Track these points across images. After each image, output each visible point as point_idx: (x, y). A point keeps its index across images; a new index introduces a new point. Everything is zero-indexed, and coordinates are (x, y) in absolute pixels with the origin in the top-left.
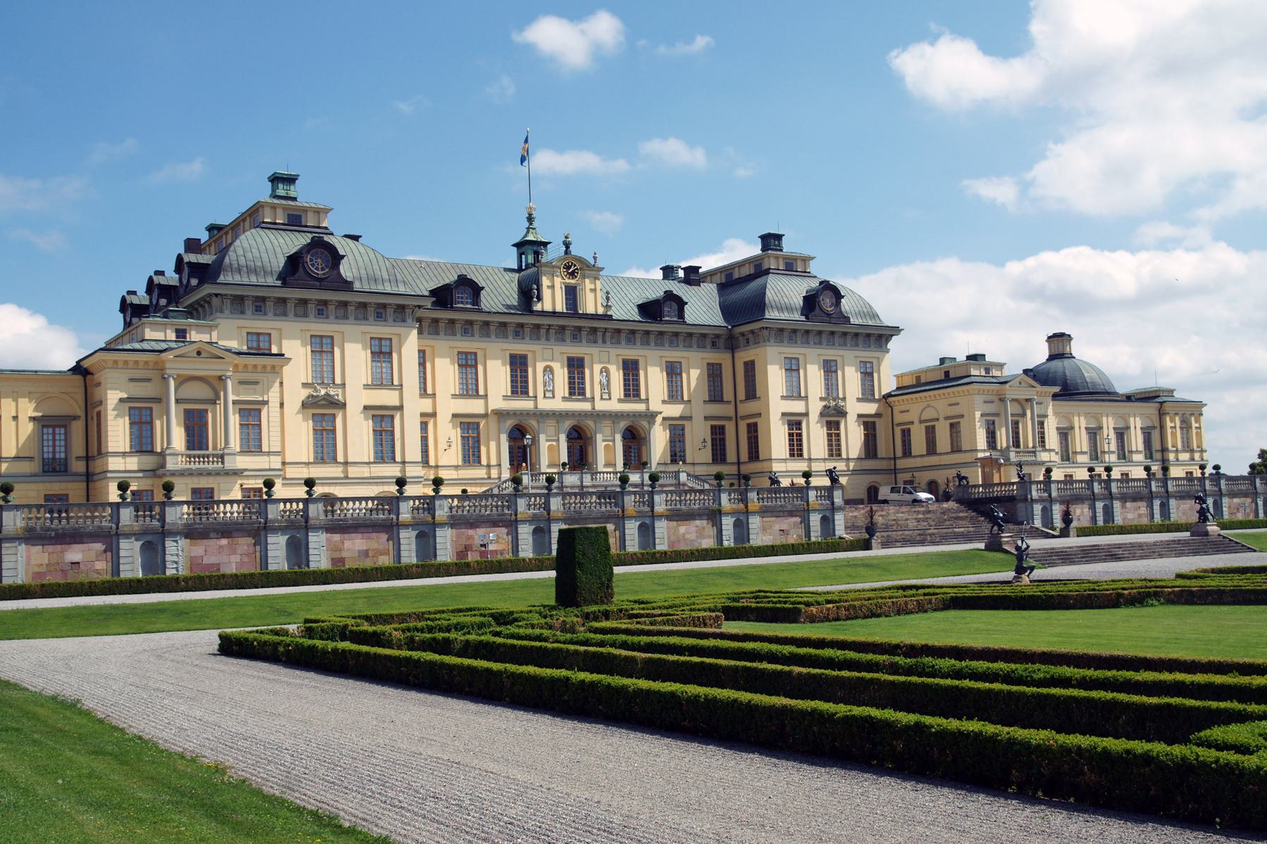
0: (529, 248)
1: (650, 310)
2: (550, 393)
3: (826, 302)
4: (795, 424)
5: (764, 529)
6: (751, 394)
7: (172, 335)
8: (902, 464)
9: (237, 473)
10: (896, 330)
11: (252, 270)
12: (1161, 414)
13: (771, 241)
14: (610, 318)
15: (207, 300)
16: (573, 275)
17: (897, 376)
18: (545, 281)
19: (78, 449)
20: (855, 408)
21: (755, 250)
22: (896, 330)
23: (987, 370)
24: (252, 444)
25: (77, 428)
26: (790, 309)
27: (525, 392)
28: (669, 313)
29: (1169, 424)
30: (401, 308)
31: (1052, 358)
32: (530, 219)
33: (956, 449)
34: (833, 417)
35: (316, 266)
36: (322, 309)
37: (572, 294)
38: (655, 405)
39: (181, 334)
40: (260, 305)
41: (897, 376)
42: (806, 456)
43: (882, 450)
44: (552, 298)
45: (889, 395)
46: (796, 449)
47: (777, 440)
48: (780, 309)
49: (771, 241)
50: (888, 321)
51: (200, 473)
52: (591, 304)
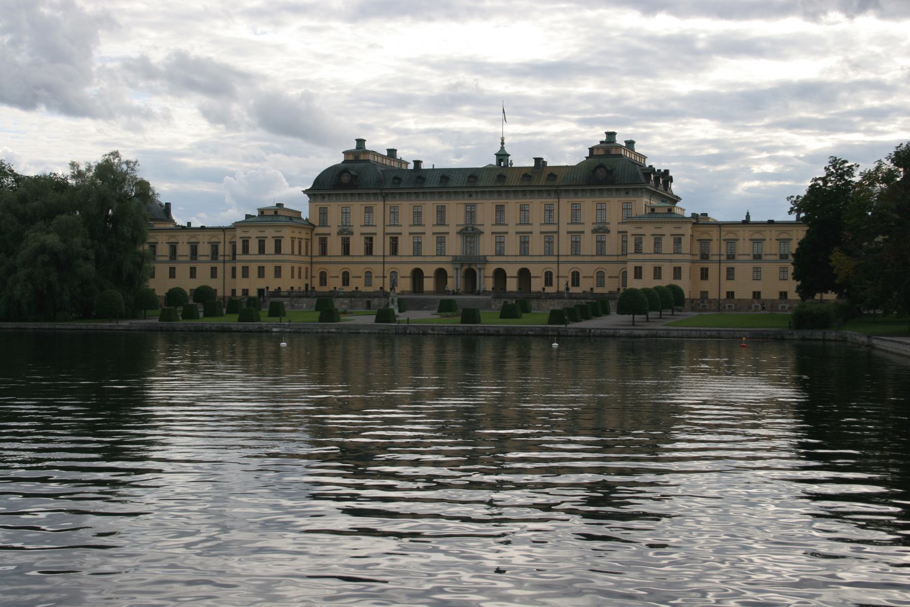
4: (575, 237)
20: (614, 228)
35: (345, 179)
40: (323, 197)
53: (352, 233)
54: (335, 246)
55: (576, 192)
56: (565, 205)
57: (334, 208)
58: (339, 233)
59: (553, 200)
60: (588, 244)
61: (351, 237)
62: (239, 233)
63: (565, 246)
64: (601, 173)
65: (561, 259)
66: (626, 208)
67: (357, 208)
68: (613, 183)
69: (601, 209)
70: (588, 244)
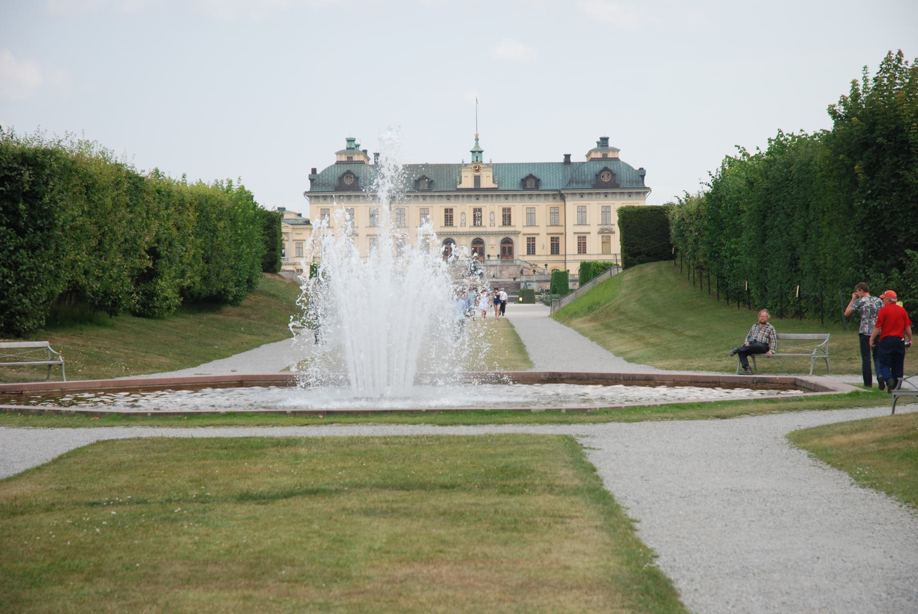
0: (477, 152)
1: (524, 182)
2: (463, 224)
11: (324, 185)
13: (604, 141)
16: (478, 171)
18: (463, 174)
26: (583, 182)
27: (451, 225)
32: (477, 140)
35: (348, 182)
36: (349, 197)
37: (477, 180)
38: (518, 229)
44: (467, 182)
47: (571, 245)
48: (577, 183)
49: (604, 141)
50: (646, 185)
52: (487, 182)
55: (582, 195)
56: (572, 205)
59: (558, 203)
64: (606, 179)
65: (568, 258)
68: (617, 186)
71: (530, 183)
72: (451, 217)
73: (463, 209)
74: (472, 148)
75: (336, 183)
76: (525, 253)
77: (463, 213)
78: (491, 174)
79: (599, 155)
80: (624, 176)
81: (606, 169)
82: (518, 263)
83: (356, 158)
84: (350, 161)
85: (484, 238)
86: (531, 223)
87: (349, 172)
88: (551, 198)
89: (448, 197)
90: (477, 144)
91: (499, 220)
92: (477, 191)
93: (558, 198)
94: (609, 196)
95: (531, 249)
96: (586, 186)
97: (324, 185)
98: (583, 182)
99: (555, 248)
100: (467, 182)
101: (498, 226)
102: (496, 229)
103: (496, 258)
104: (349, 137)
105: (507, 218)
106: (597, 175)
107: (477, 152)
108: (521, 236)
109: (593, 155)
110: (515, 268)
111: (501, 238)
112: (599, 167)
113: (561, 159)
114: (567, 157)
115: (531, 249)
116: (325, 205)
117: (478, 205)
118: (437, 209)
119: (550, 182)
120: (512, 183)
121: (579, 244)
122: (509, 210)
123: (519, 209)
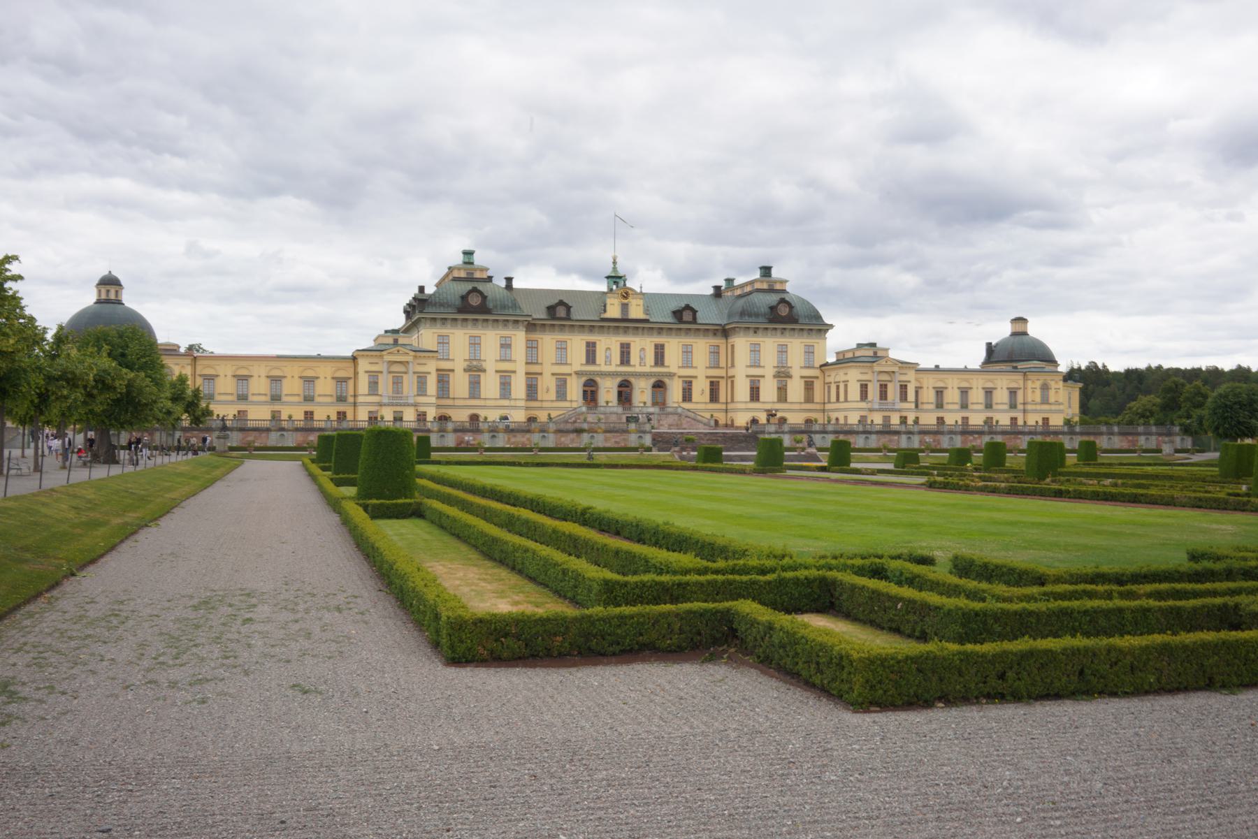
1: (678, 314)
2: (608, 361)
3: (783, 311)
5: (606, 440)
6: (733, 366)
7: (391, 341)
8: (828, 406)
9: (415, 405)
10: (831, 326)
11: (442, 305)
12: (1025, 380)
13: (766, 271)
14: (646, 321)
15: (419, 320)
17: (837, 353)
18: (609, 301)
19: (351, 392)
20: (797, 371)
21: (757, 275)
22: (831, 326)
23: (875, 353)
24: (422, 391)
25: (351, 383)
26: (757, 315)
28: (687, 316)
29: (1030, 384)
30: (516, 322)
31: (1014, 334)
32: (615, 263)
33: (846, 400)
34: (783, 375)
35: (475, 301)
37: (625, 307)
39: (396, 341)
41: (837, 353)
42: (762, 399)
43: (818, 396)
45: (826, 364)
46: (755, 394)
48: (750, 315)
50: (827, 321)
51: (397, 405)
52: (636, 312)
53: (485, 371)
54: (460, 385)
55: (756, 331)
56: (742, 344)
57: (459, 338)
58: (468, 370)
60: (769, 391)
61: (482, 374)
62: (363, 365)
63: (742, 392)
66: (809, 351)
67: (490, 338)
68: (795, 321)
69: (783, 350)
70: (769, 391)
71: (684, 316)
72: (594, 352)
73: (609, 345)
74: (609, 272)
75: (458, 302)
76: (681, 399)
77: (608, 349)
78: (641, 302)
79: (765, 286)
80: (799, 309)
81: (783, 301)
82: (680, 410)
83: (478, 275)
84: (470, 279)
85: (632, 380)
86: (688, 364)
87: (475, 290)
88: (711, 334)
89: (592, 329)
90: (615, 269)
91: (650, 358)
92: (625, 324)
93: (719, 334)
94: (787, 333)
95: (687, 396)
96: (761, 320)
97: (442, 305)
98: (757, 315)
99: (714, 397)
100: (614, 311)
101: (649, 365)
102: (647, 369)
103: (649, 403)
104: (467, 248)
105: (659, 357)
106: (772, 308)
107: (615, 278)
108: (676, 378)
109: (758, 286)
110: (676, 417)
111: (653, 380)
112: (773, 299)
113: (711, 291)
114: (717, 288)
115: (687, 396)
116: (444, 331)
117: (625, 339)
118: (577, 344)
119: (708, 315)
120: (663, 316)
121: (752, 388)
122: (662, 346)
123: (674, 347)
